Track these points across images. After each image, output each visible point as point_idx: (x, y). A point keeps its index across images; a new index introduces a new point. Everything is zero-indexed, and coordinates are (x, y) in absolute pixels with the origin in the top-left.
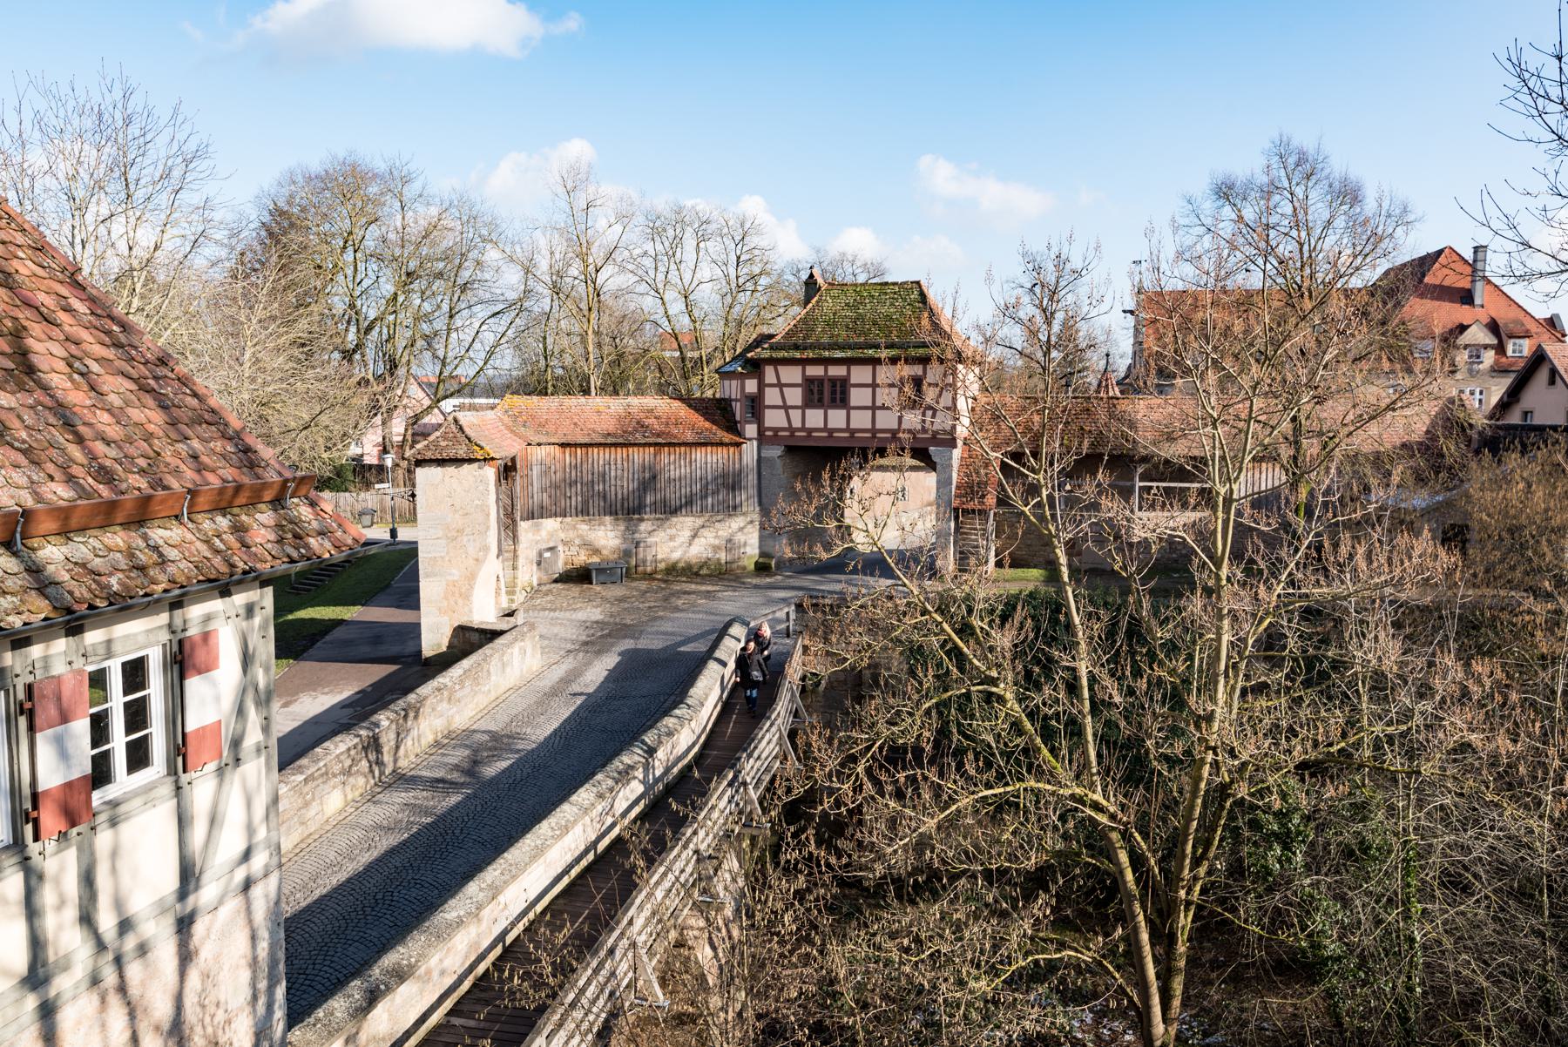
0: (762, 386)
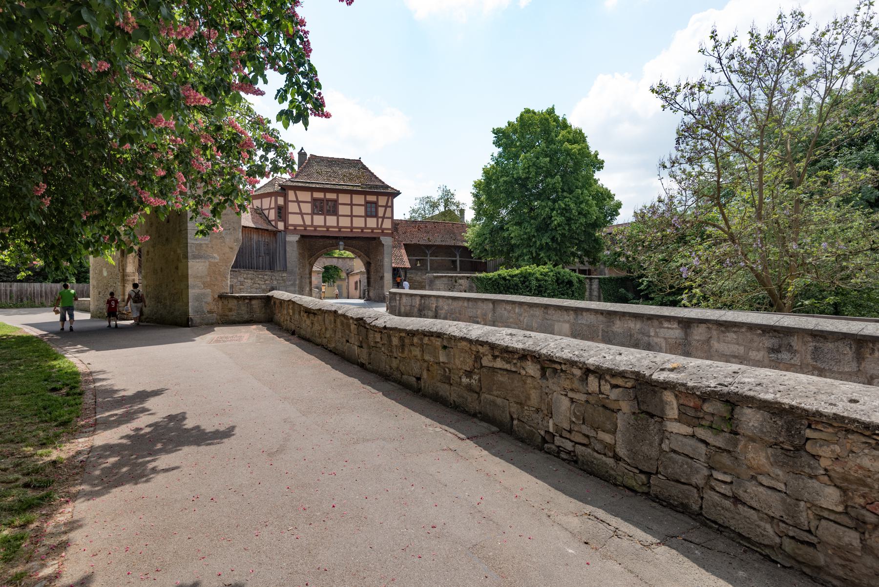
0: (286, 201)
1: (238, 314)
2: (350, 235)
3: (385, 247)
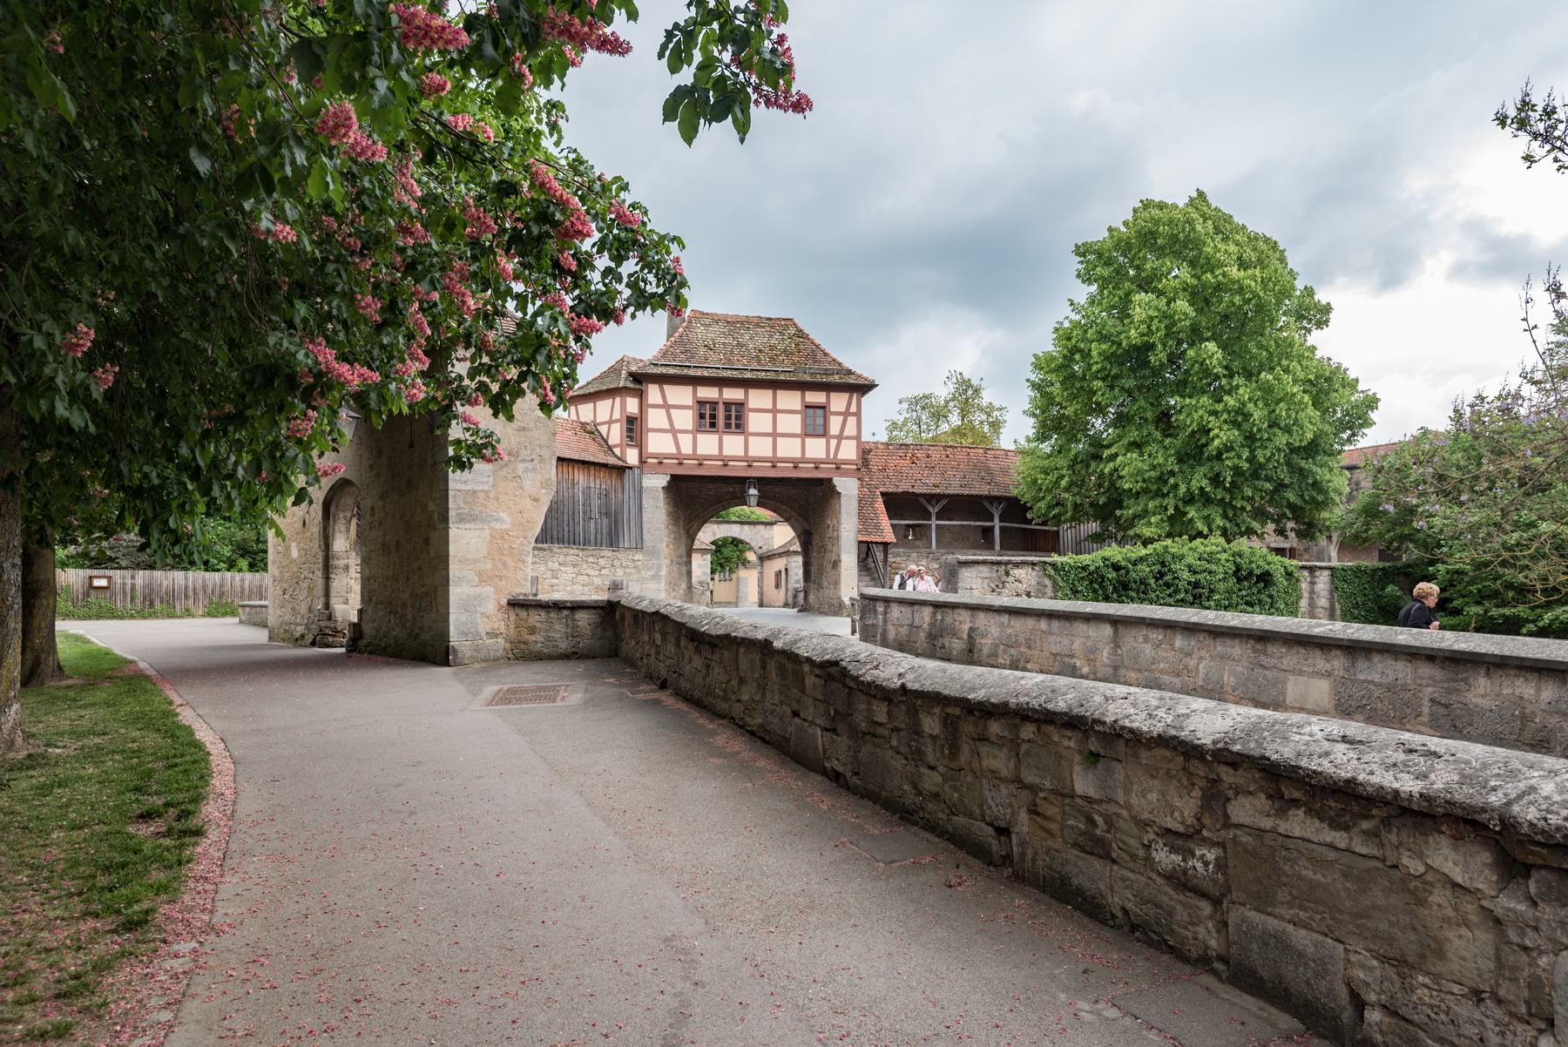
1: (548, 639)
2: (772, 474)
3: (843, 500)
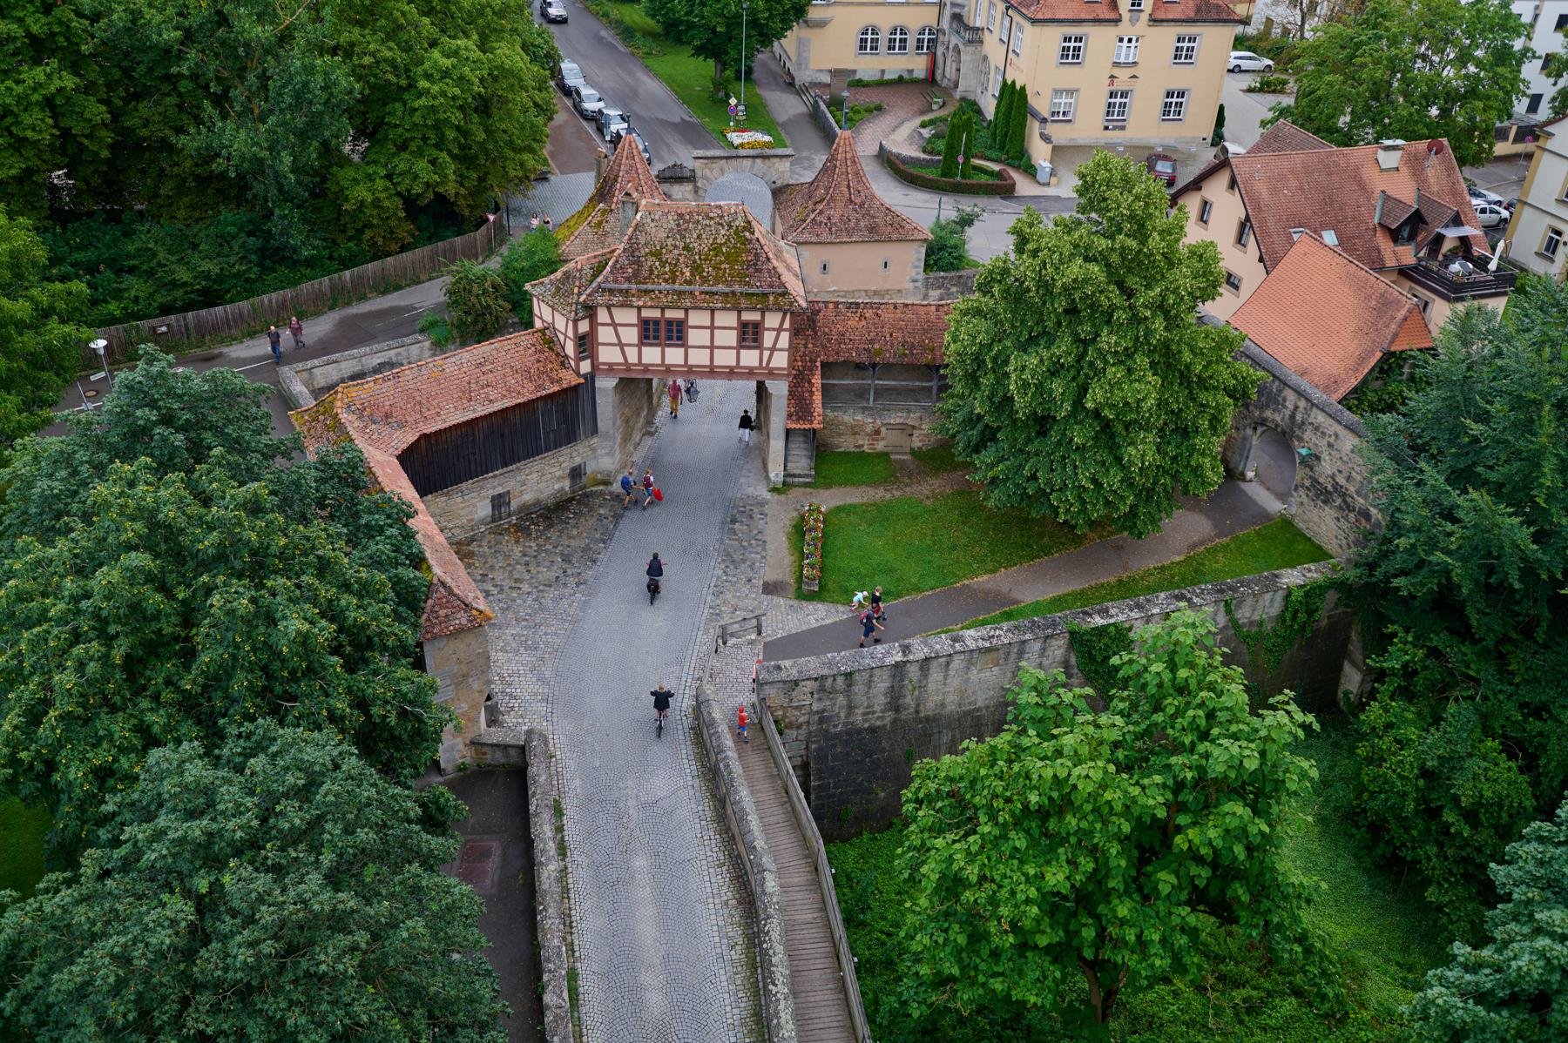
0: (594, 324)
